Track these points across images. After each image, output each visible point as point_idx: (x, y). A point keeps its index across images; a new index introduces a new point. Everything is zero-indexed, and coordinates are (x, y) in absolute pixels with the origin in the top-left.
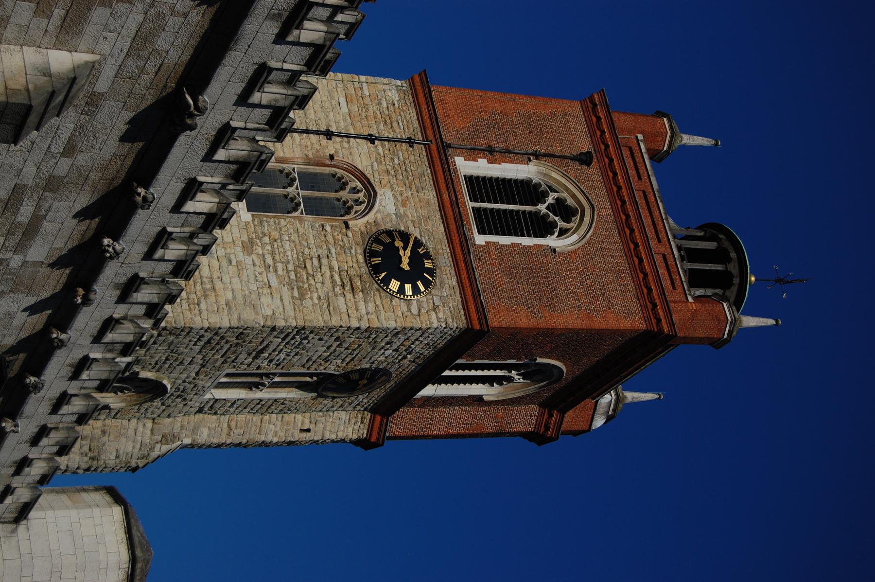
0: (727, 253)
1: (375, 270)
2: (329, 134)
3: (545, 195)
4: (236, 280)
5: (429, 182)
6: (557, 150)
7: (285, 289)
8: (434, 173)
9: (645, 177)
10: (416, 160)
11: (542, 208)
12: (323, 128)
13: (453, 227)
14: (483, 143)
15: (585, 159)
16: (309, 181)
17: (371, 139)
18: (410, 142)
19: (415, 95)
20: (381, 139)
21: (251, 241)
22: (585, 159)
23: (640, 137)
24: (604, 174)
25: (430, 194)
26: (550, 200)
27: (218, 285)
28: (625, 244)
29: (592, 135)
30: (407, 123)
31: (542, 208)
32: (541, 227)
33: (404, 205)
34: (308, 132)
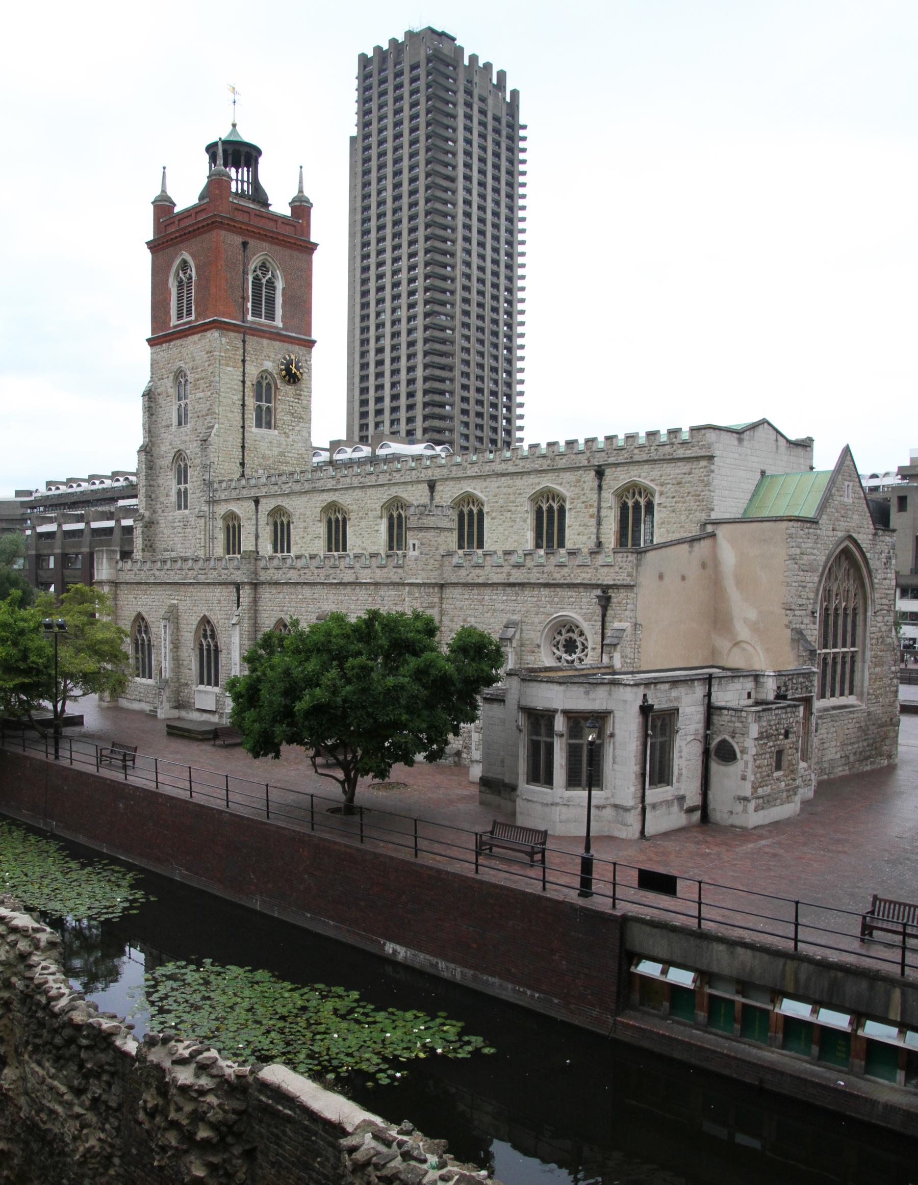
0: (247, 152)
1: (294, 382)
2: (244, 382)
3: (257, 275)
4: (299, 444)
5: (260, 340)
6: (240, 257)
7: (301, 424)
8: (257, 336)
9: (249, 210)
10: (251, 341)
11: (264, 281)
12: (241, 384)
13: (279, 338)
14: (240, 300)
15: (245, 244)
16: (259, 398)
17: (244, 361)
18: (244, 341)
19: (224, 329)
20: (244, 356)
21: (285, 433)
22: (245, 244)
23: (231, 199)
24: (251, 237)
25: (265, 342)
26: (259, 272)
27: (300, 452)
28: (280, 245)
29: (233, 232)
30: (235, 338)
31: (264, 281)
32: (271, 284)
33: (269, 357)
34: (244, 392)
